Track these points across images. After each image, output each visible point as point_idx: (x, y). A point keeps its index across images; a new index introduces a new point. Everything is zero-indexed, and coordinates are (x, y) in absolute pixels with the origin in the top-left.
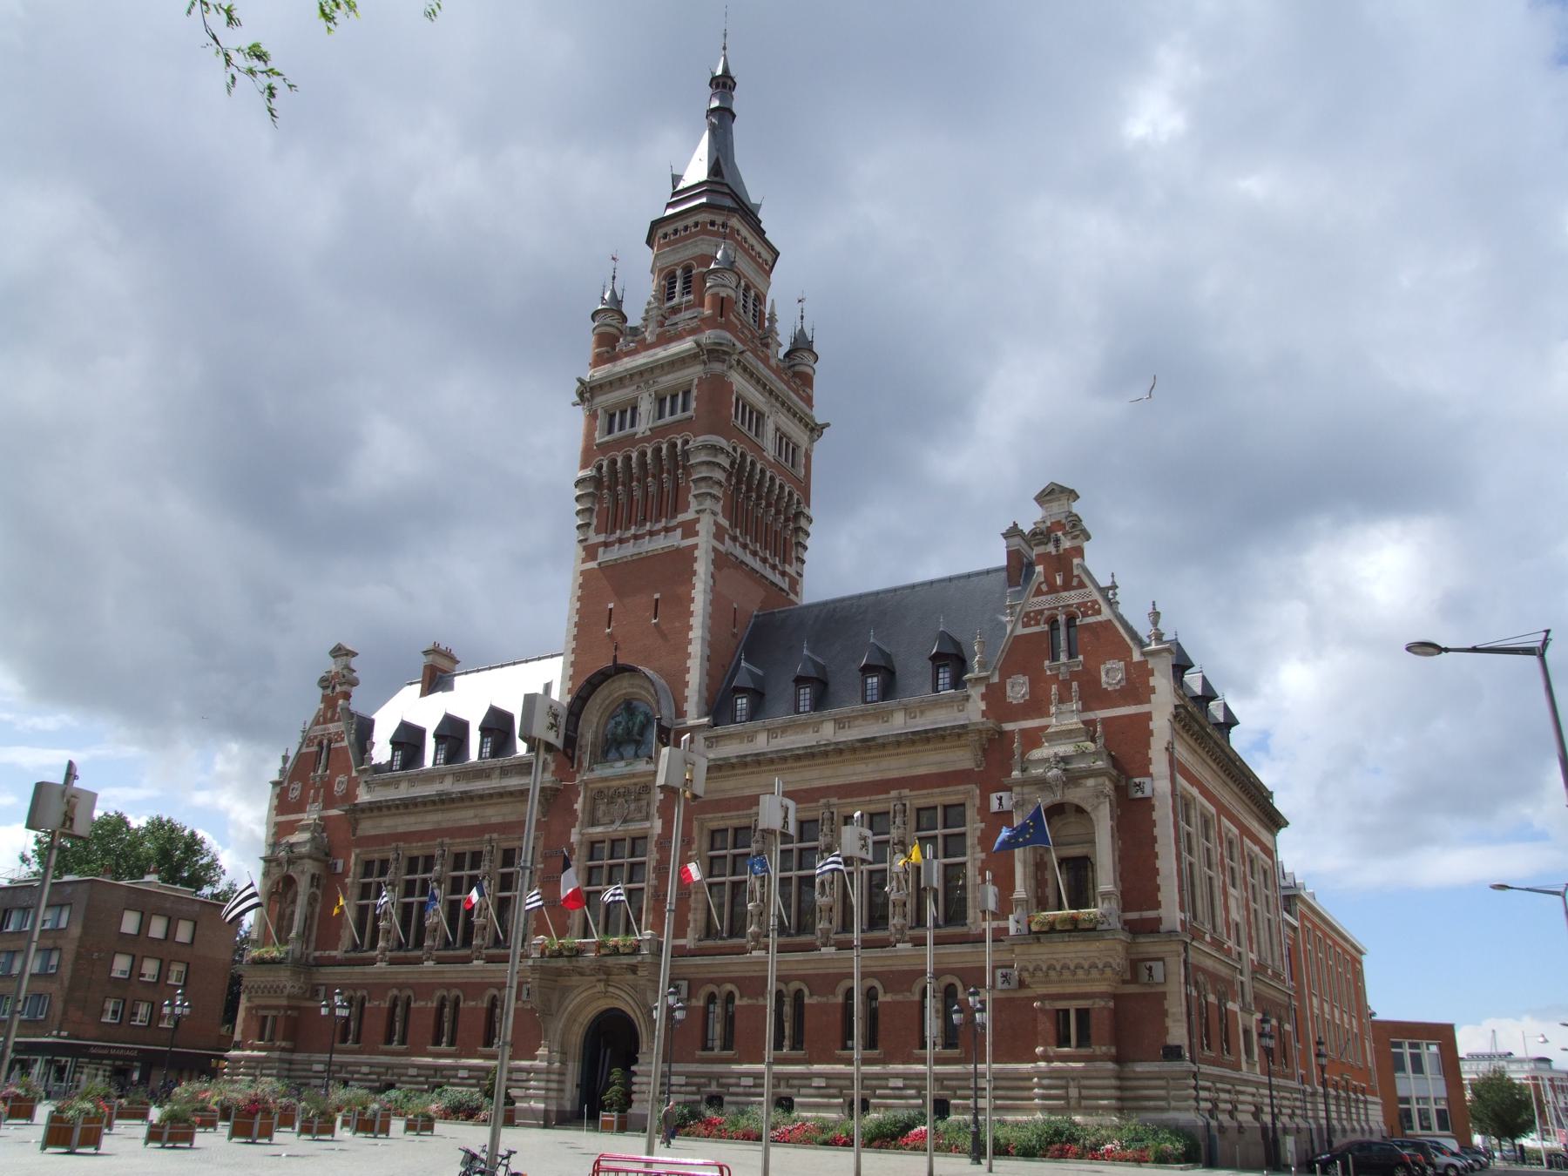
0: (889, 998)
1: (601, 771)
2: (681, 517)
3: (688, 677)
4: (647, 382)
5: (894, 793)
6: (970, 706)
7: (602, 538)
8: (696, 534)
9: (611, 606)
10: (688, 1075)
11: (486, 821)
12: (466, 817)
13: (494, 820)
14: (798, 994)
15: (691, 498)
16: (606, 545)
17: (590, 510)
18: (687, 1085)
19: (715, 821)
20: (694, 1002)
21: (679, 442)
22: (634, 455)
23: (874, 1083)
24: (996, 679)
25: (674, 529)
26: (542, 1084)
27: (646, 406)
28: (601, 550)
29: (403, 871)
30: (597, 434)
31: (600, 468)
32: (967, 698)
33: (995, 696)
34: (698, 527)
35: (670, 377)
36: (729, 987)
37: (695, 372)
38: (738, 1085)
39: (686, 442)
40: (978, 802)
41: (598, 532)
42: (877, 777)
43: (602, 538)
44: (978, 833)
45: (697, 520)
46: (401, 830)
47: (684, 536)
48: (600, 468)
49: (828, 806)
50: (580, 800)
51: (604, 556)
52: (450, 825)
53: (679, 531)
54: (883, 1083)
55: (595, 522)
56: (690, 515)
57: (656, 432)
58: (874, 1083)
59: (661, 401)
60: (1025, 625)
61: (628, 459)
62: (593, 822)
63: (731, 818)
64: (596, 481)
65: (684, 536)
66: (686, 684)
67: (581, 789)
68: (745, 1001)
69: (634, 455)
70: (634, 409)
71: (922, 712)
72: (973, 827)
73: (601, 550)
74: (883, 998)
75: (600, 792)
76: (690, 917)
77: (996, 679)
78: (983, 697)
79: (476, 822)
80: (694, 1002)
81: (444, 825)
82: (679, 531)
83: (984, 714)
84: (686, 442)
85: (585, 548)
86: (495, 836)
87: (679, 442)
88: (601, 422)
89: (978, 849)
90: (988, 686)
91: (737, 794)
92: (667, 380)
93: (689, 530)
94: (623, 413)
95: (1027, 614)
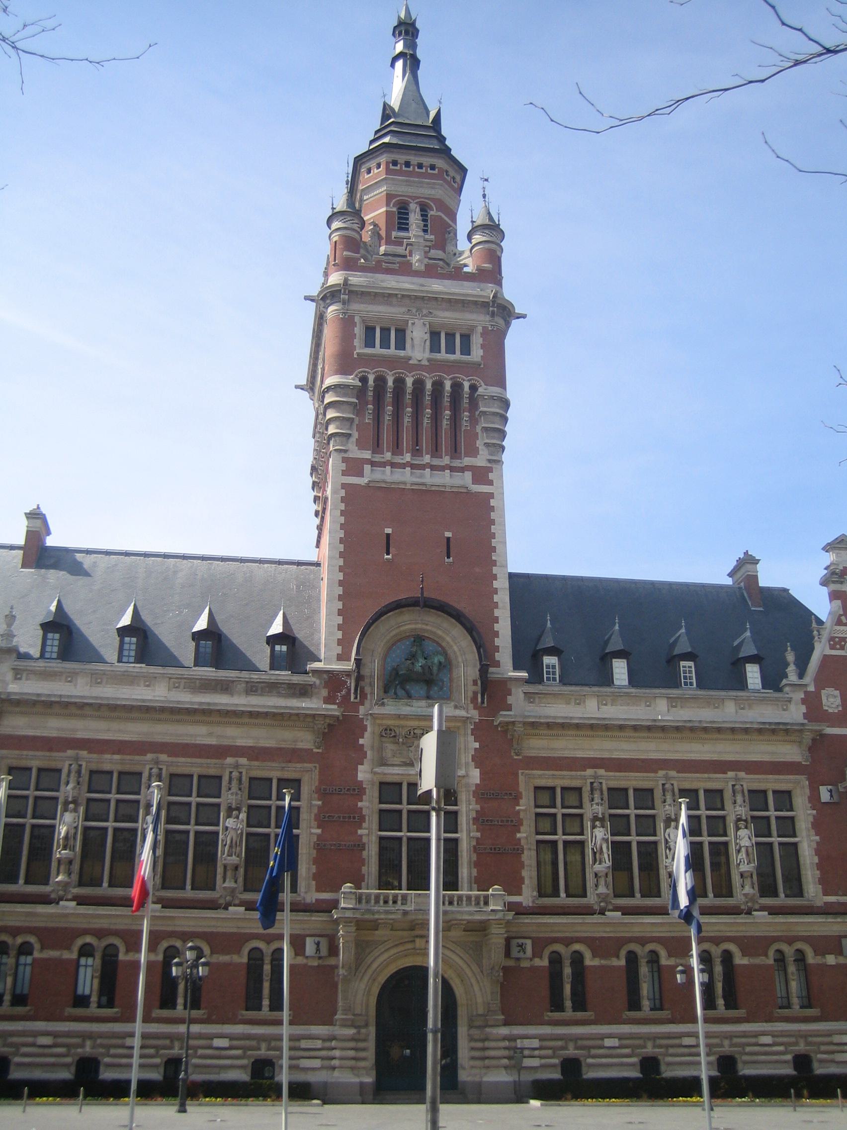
0: (745, 961)
1: (391, 708)
2: (467, 461)
3: (496, 627)
4: (419, 310)
5: (731, 774)
6: (792, 707)
7: (367, 455)
8: (491, 483)
9: (388, 531)
10: (542, 1038)
11: (226, 742)
12: (199, 733)
13: (240, 742)
14: (727, 957)
15: (479, 443)
16: (373, 464)
17: (351, 420)
18: (541, 1048)
19: (545, 778)
20: (537, 962)
21: (466, 385)
22: (409, 381)
23: (744, 1040)
24: (811, 688)
25: (462, 470)
26: (352, 1053)
27: (418, 334)
28: (367, 468)
29: (85, 787)
30: (356, 342)
31: (364, 380)
32: (790, 700)
33: (812, 703)
34: (491, 476)
35: (447, 314)
36: (577, 947)
37: (480, 320)
38: (602, 1047)
39: (473, 388)
40: (807, 791)
41: (361, 445)
42: (715, 757)
43: (367, 455)
44: (811, 819)
45: (490, 470)
46: (79, 735)
47: (476, 481)
48: (364, 380)
49: (667, 777)
50: (367, 735)
51: (369, 475)
52: (167, 739)
53: (468, 475)
54: (753, 1040)
55: (356, 435)
56: (480, 461)
57: (434, 366)
58: (744, 1040)
59: (434, 335)
60: (832, 648)
61: (400, 382)
62: (383, 763)
63: (563, 777)
64: (361, 392)
65: (476, 481)
66: (496, 634)
67: (368, 723)
68: (596, 962)
69: (409, 381)
70: (401, 333)
71: (750, 707)
72: (803, 814)
73: (367, 468)
74: (740, 960)
75: (388, 729)
76: (525, 873)
77: (811, 688)
78: (804, 701)
79: (213, 741)
80: (537, 962)
81: (159, 739)
82: (468, 475)
83: (806, 716)
84: (473, 388)
85: (344, 460)
86: (243, 761)
87: (466, 385)
88: (359, 331)
89: (813, 832)
90: (806, 693)
91: (567, 754)
92: (446, 317)
93: (482, 475)
94: (385, 331)
95: (832, 639)
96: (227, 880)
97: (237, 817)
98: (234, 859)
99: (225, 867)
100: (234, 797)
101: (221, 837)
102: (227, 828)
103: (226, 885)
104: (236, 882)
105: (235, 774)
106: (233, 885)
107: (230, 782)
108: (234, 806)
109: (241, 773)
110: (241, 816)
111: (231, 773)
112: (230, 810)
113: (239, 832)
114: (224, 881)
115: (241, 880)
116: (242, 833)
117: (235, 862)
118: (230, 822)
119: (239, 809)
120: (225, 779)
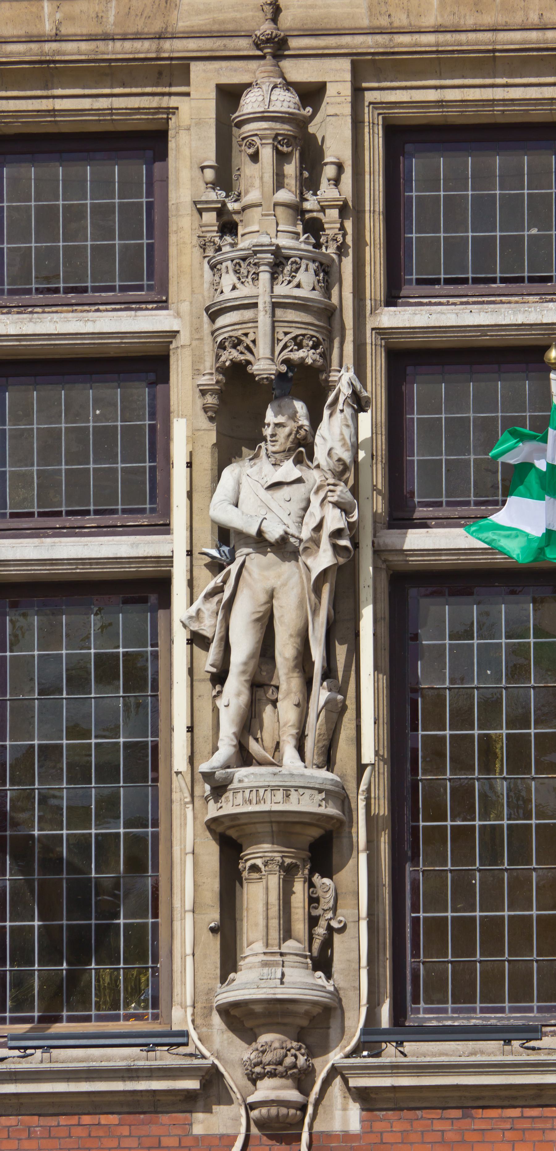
96: (253, 945)
97: (302, 449)
98: (287, 781)
99: (230, 840)
100: (261, 290)
101: (180, 606)
102: (225, 535)
103: (251, 983)
104: (322, 963)
105: (265, 98)
106: (300, 983)
107: (224, 177)
108: (263, 366)
109: (311, 94)
110: (332, 435)
111: (229, 96)
112: (241, 407)
113: (323, 559)
114: (229, 963)
115: (354, 949)
116: (341, 584)
117: (307, 804)
118: (254, 493)
119: (308, 384)
120: (192, 146)
